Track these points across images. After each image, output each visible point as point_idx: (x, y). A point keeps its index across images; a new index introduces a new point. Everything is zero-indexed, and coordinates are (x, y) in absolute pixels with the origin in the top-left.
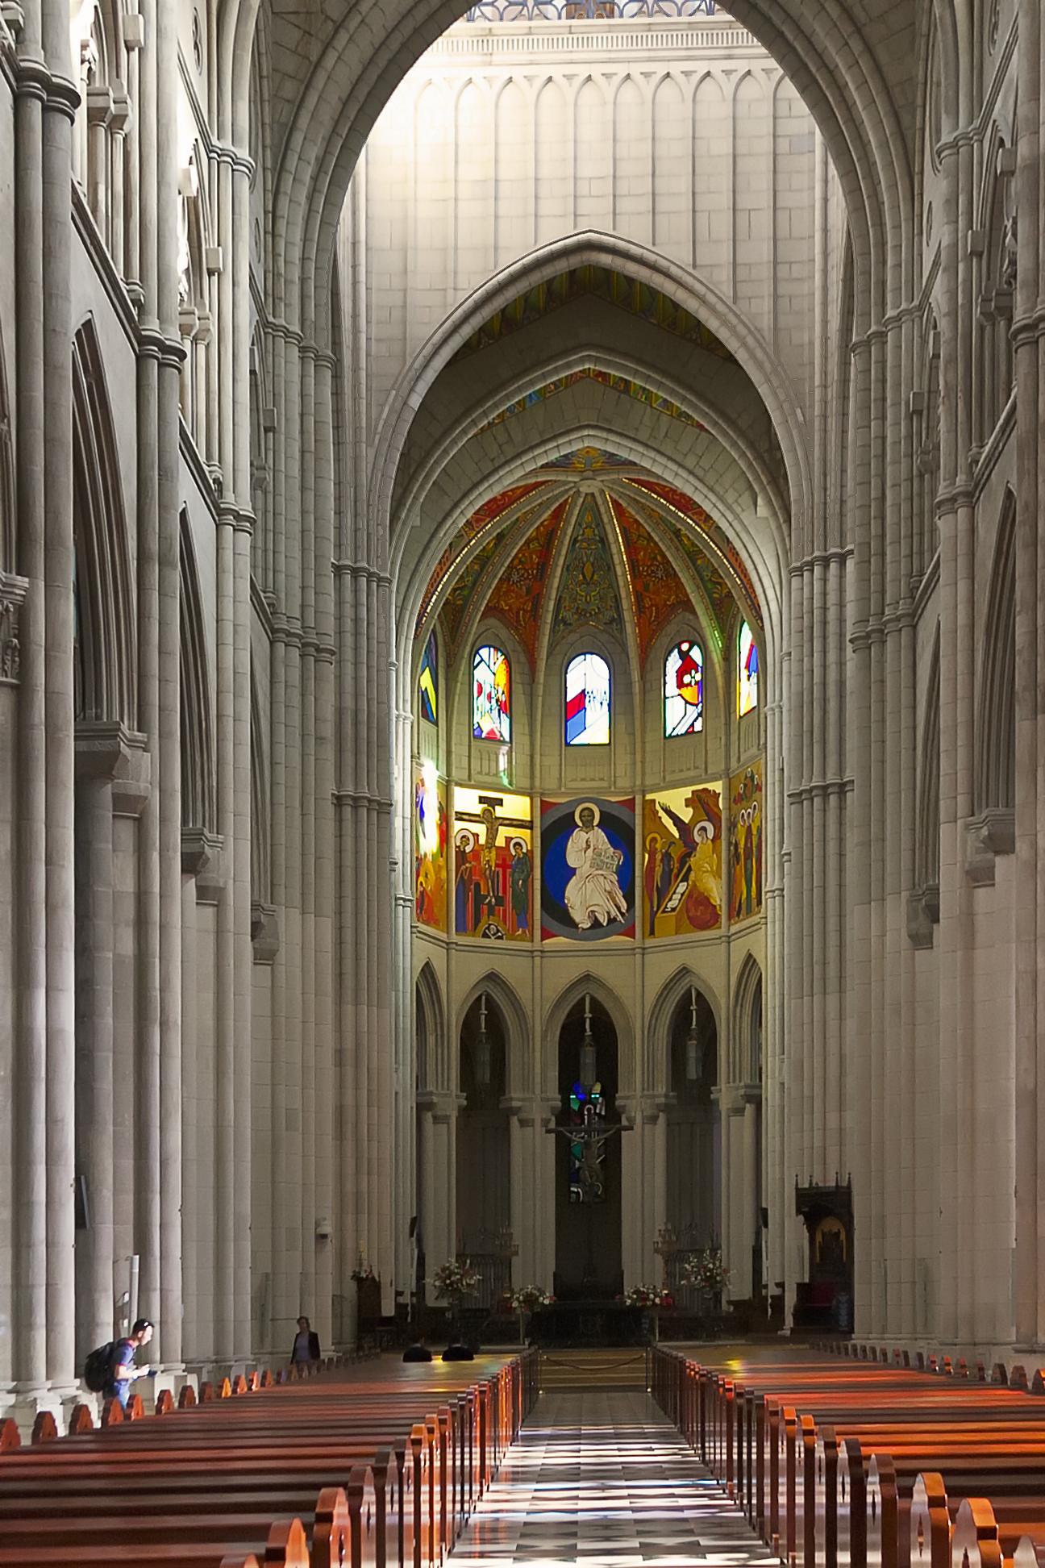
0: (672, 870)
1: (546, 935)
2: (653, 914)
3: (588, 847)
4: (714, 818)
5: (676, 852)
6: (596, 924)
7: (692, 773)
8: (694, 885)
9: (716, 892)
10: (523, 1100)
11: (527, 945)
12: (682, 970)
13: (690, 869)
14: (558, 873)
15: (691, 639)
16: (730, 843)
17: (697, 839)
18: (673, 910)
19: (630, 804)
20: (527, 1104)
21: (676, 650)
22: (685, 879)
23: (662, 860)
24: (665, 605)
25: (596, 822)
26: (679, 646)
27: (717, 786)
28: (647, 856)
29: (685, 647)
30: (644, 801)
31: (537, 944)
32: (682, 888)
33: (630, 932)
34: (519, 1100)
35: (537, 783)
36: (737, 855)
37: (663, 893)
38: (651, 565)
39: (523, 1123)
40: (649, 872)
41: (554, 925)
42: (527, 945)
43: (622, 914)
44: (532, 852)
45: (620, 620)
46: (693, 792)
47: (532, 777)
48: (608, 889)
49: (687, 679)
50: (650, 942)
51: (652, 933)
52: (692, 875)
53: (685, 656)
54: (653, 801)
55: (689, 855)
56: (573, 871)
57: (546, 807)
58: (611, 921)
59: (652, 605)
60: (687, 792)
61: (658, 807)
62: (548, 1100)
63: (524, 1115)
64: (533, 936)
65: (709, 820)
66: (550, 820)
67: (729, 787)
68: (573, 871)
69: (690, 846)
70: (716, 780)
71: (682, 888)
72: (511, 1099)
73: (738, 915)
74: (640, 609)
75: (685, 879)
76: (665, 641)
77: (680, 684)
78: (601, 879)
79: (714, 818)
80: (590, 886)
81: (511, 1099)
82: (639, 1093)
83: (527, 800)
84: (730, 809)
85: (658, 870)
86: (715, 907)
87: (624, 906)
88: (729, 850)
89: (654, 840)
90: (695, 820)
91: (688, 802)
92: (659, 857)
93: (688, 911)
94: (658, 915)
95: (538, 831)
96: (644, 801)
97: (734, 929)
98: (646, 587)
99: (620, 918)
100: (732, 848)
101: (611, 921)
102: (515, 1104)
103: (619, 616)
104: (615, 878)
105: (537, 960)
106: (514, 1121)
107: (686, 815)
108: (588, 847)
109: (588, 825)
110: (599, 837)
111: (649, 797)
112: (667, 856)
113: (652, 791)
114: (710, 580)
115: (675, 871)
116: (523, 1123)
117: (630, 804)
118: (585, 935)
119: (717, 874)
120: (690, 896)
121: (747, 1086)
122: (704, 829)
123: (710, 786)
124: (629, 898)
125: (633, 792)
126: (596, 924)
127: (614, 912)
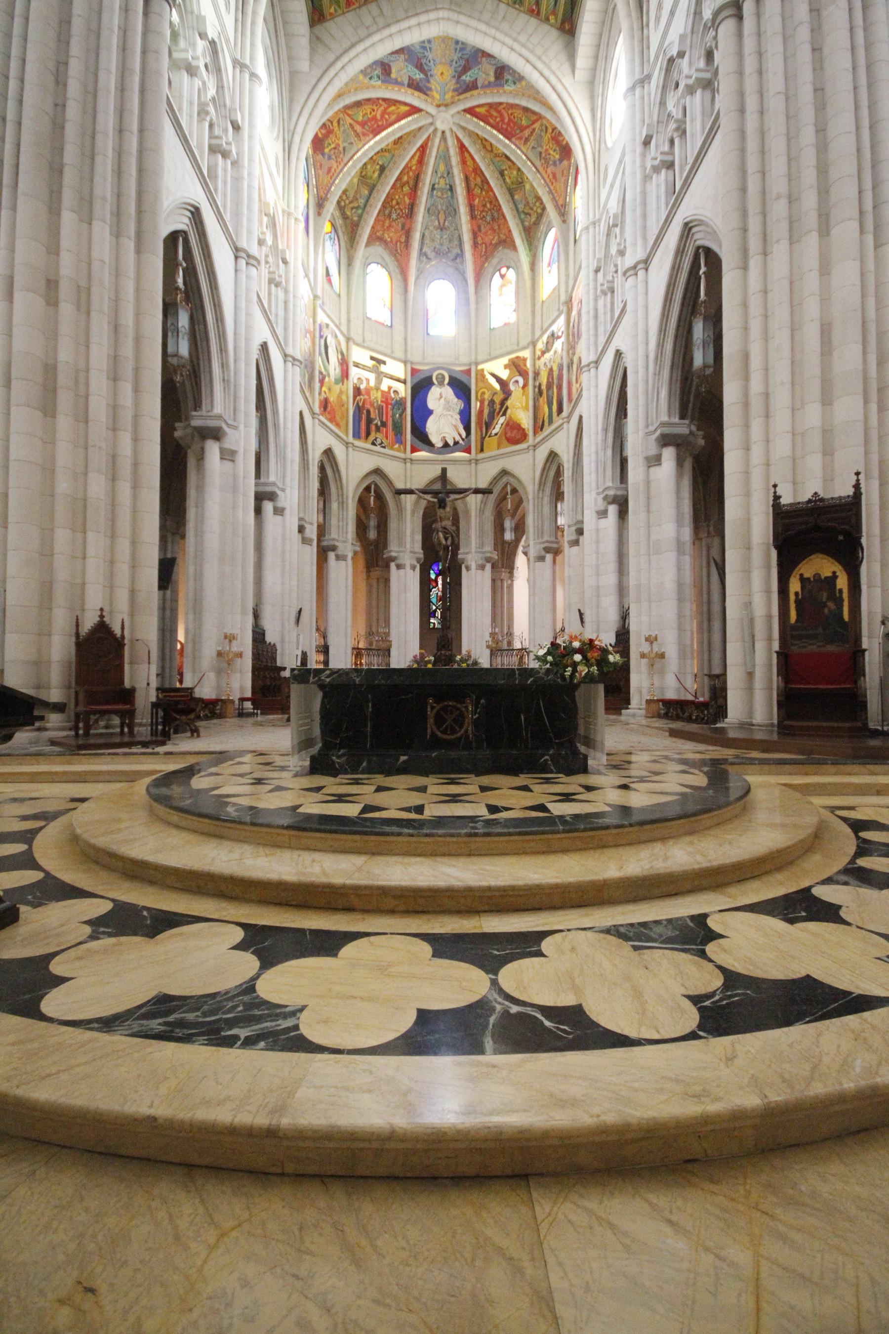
0: (494, 410)
1: (414, 450)
2: (483, 439)
3: (441, 397)
4: (523, 373)
5: (498, 399)
6: (446, 445)
7: (509, 349)
8: (510, 417)
9: (525, 420)
10: (398, 552)
11: (402, 455)
12: (501, 473)
13: (507, 408)
14: (421, 413)
15: (508, 264)
16: (535, 387)
17: (512, 387)
18: (496, 434)
19: (468, 372)
20: (401, 554)
21: (498, 273)
22: (504, 414)
23: (489, 405)
24: (491, 244)
25: (447, 381)
26: (499, 270)
27: (526, 354)
28: (478, 404)
29: (504, 270)
30: (477, 371)
31: (409, 454)
32: (502, 420)
33: (468, 450)
34: (395, 552)
35: (409, 356)
36: (540, 393)
37: (489, 425)
38: (483, 211)
39: (399, 567)
40: (480, 412)
41: (419, 444)
42: (402, 455)
43: (463, 440)
44: (405, 398)
45: (461, 255)
46: (509, 360)
47: (406, 351)
48: (454, 423)
49: (504, 289)
50: (481, 456)
51: (482, 450)
52: (509, 412)
53: (503, 276)
54: (482, 370)
55: (506, 399)
56: (431, 412)
57: (414, 372)
58: (456, 443)
59: (482, 244)
60: (505, 360)
61: (486, 373)
62: (415, 553)
63: (398, 562)
64: (405, 449)
65: (520, 375)
66: (416, 380)
67: (534, 352)
68: (431, 412)
69: (507, 393)
70: (524, 348)
71: (502, 420)
72: (390, 551)
73: (542, 429)
74: (475, 245)
75: (504, 414)
76: (491, 270)
77: (501, 295)
78: (449, 417)
79: (523, 373)
80: (442, 421)
81: (390, 551)
82: (473, 550)
83: (402, 365)
84: (534, 365)
85: (486, 411)
86: (524, 430)
87: (464, 434)
88: (534, 391)
89: (483, 393)
90: (510, 378)
91: (506, 367)
92: (486, 403)
93: (506, 434)
94: (487, 439)
95: (409, 385)
96: (477, 371)
97: (538, 440)
98: (480, 230)
99: (461, 442)
100: (537, 390)
101: (456, 443)
102: (393, 554)
103: (462, 251)
104: (458, 417)
105: (408, 464)
106: (393, 566)
107: (504, 374)
108: (441, 397)
109: (441, 383)
110: (448, 392)
111: (480, 367)
112: (492, 402)
113: (482, 362)
114: (523, 212)
115: (497, 410)
116: (399, 567)
117: (468, 372)
118: (439, 451)
119: (527, 408)
120: (507, 424)
121: (547, 542)
122: (517, 382)
123: (521, 354)
124: (467, 429)
125: (470, 364)
126: (446, 445)
127: (458, 438)
